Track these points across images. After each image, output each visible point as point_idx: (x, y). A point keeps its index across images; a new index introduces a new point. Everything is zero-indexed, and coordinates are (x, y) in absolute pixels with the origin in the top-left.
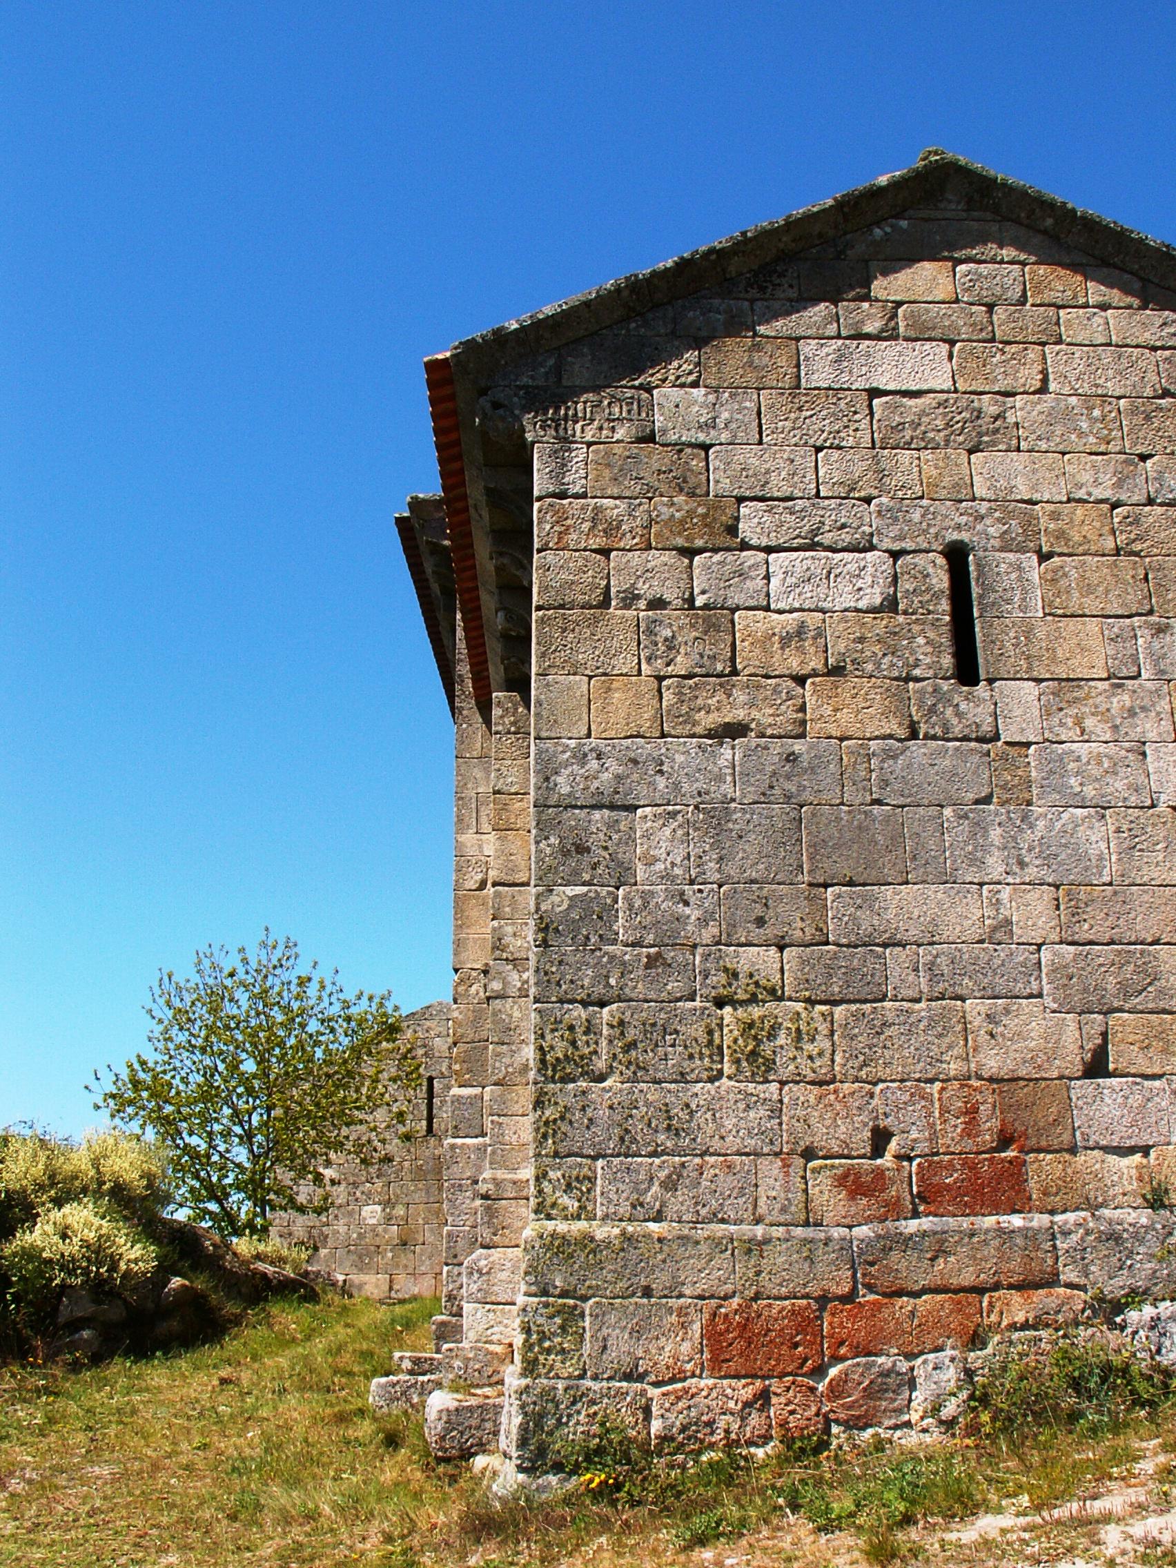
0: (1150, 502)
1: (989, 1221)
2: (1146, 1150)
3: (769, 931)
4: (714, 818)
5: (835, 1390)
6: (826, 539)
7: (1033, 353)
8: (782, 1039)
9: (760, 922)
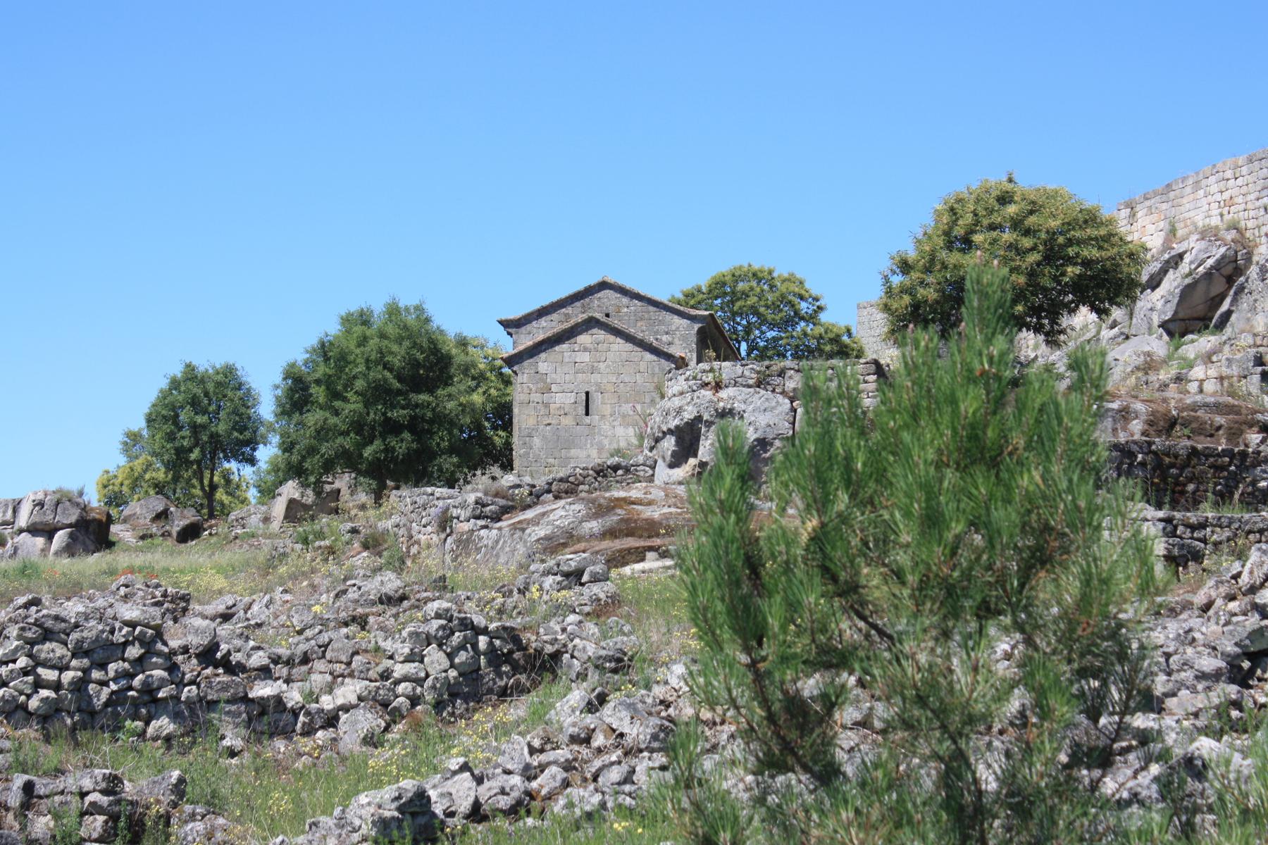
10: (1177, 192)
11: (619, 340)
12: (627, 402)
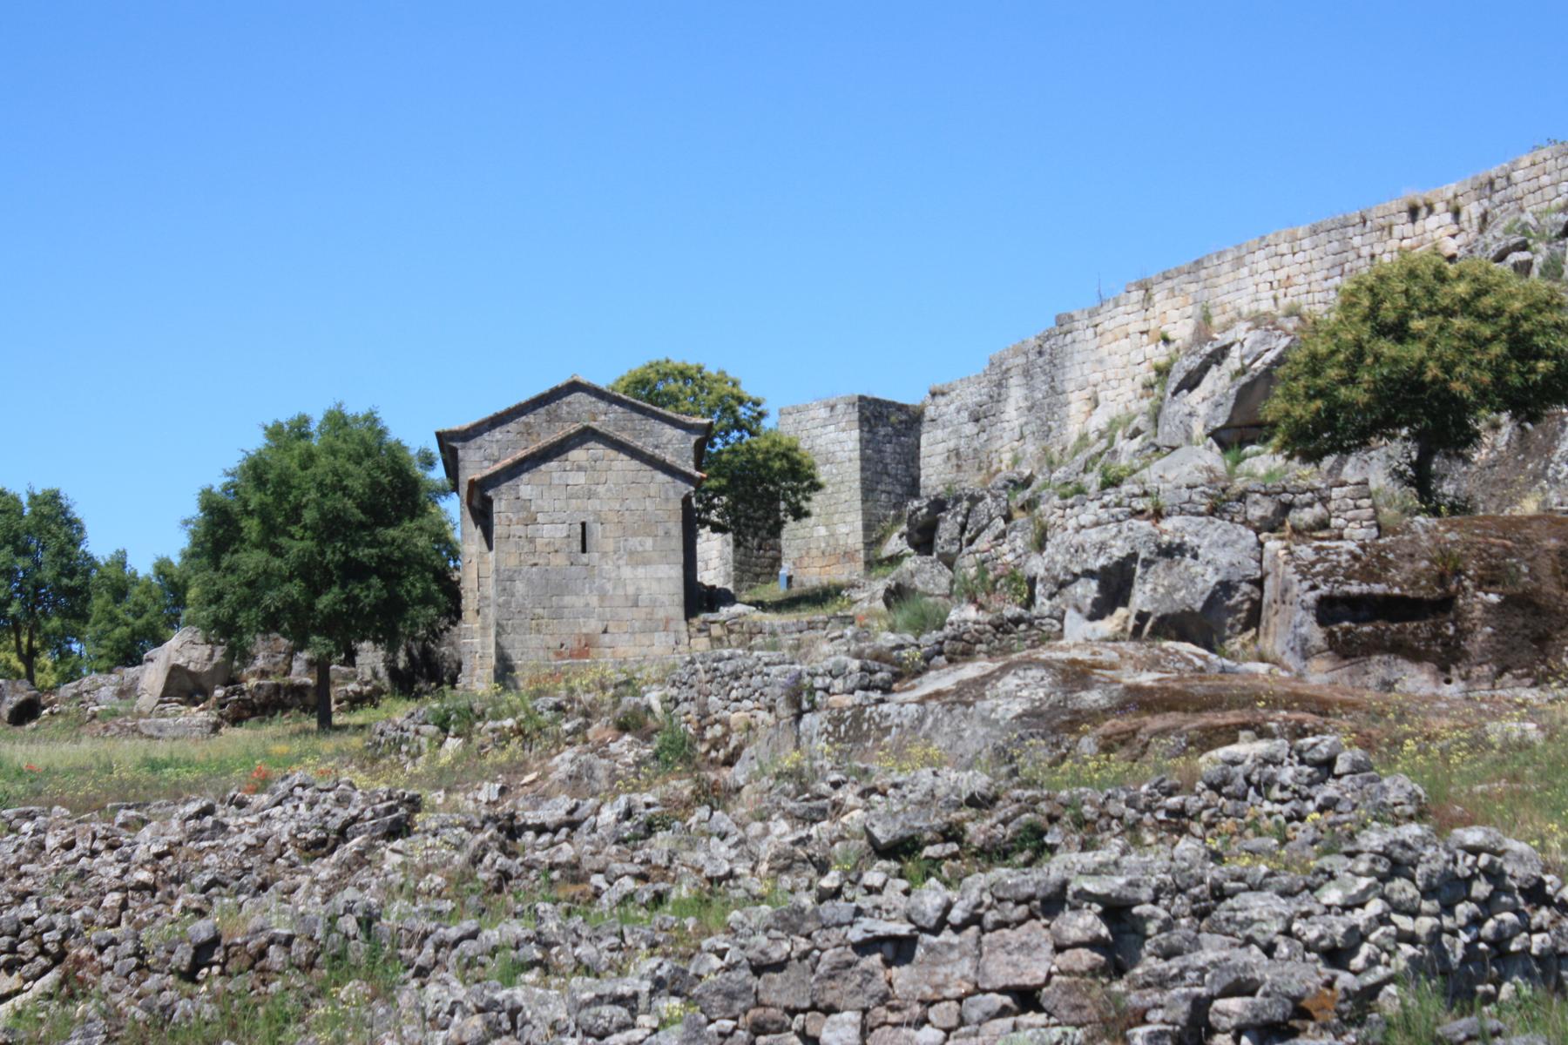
4: (530, 582)
10: (1211, 270)
11: (622, 456)
12: (635, 534)
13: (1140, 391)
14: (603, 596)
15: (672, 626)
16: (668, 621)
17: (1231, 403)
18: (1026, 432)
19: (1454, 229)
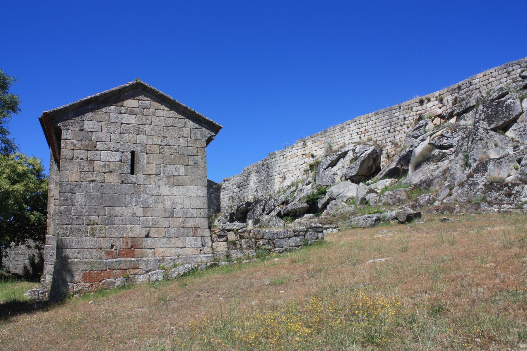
0: (166, 145)
1: (128, 259)
2: (154, 249)
3: (96, 214)
4: (88, 194)
5: (103, 284)
6: (111, 149)
7: (150, 118)
8: (97, 231)
9: (95, 212)
10: (331, 132)
11: (163, 107)
12: (171, 164)
13: (303, 173)
14: (146, 208)
15: (199, 232)
16: (196, 228)
17: (358, 167)
18: (258, 189)
19: (441, 105)
